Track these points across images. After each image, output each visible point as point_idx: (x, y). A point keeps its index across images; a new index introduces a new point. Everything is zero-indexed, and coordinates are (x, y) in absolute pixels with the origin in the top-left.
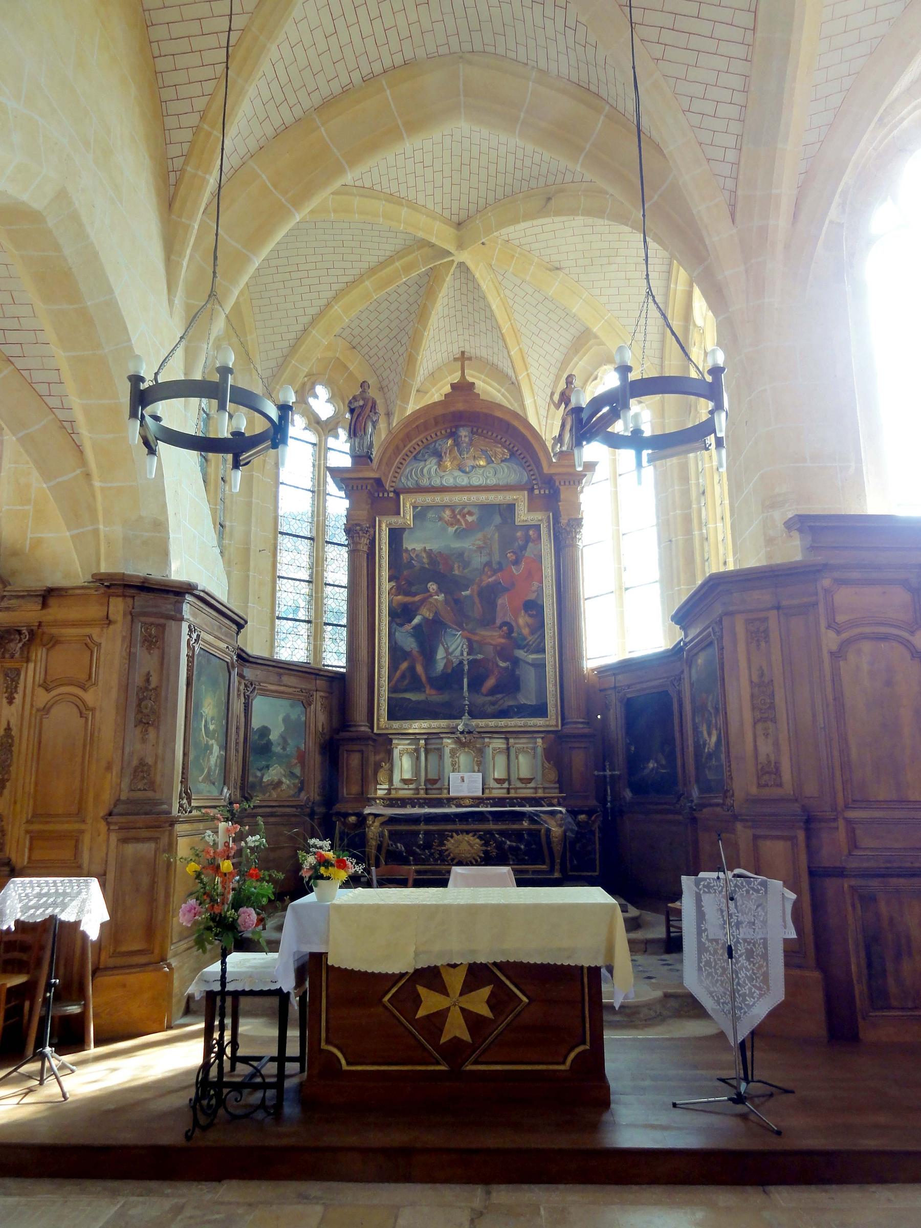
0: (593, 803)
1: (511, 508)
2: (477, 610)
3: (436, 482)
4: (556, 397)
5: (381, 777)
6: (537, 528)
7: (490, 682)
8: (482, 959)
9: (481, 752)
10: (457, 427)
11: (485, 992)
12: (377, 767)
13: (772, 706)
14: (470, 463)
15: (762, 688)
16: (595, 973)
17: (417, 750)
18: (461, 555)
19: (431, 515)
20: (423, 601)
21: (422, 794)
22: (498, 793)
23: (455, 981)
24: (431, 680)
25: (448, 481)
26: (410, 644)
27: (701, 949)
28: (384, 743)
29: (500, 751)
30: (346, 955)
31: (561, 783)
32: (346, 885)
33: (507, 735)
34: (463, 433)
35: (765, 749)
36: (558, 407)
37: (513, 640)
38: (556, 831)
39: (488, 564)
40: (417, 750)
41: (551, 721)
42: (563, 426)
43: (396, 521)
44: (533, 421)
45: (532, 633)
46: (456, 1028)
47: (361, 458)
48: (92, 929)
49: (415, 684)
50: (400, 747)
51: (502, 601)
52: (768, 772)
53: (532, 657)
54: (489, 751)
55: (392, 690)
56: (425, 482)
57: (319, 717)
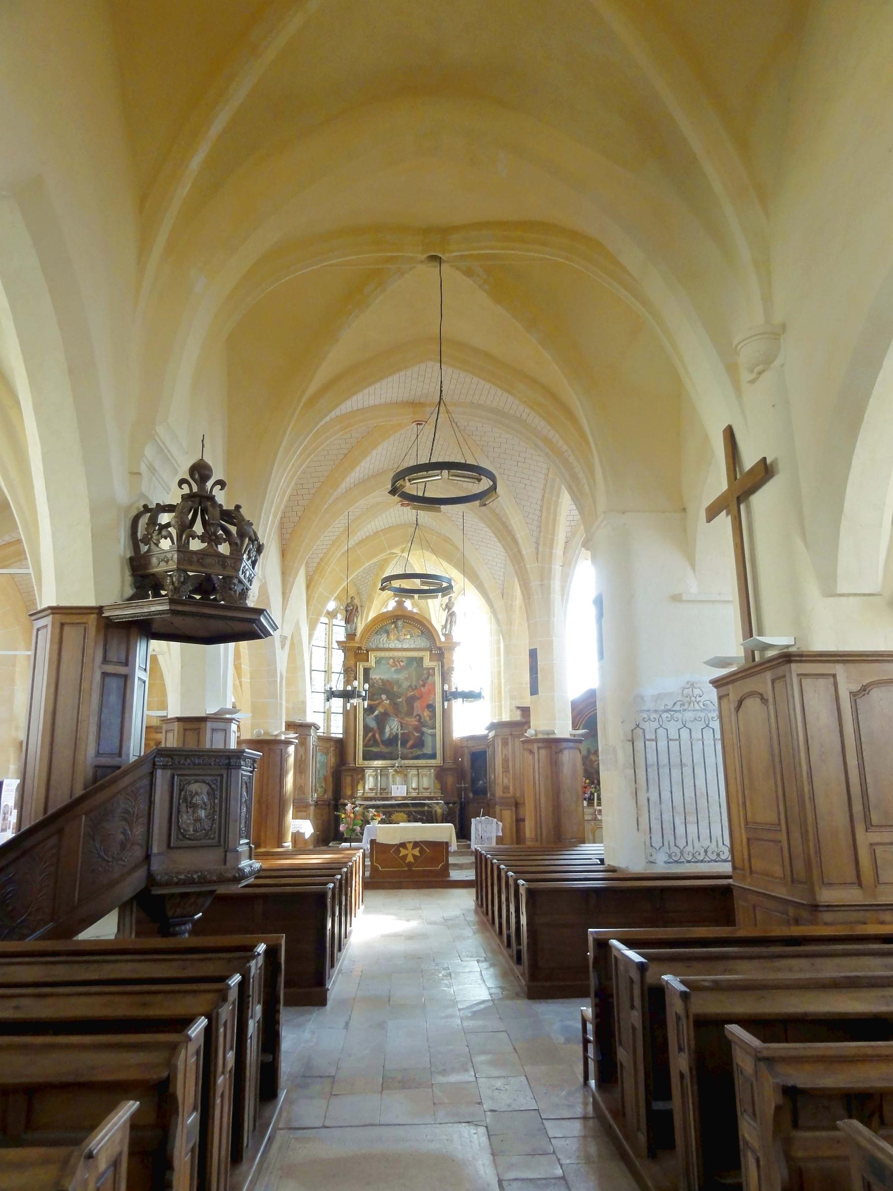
0: (456, 799)
1: (421, 659)
2: (404, 708)
3: (386, 646)
4: (444, 606)
5: (360, 787)
6: (434, 669)
7: (411, 743)
8: (417, 840)
9: (406, 776)
10: (398, 619)
11: (418, 849)
12: (358, 783)
13: (508, 767)
14: (402, 637)
15: (505, 761)
16: (447, 843)
17: (376, 775)
18: (397, 682)
19: (383, 661)
20: (379, 704)
21: (379, 795)
22: (414, 794)
23: (410, 846)
24: (383, 742)
25: (392, 645)
26: (373, 724)
27: (476, 838)
28: (362, 770)
29: (413, 775)
30: (380, 840)
31: (443, 789)
32: (380, 822)
33: (418, 768)
34: (400, 623)
35: (506, 781)
36: (444, 610)
37: (421, 723)
38: (439, 811)
39: (410, 686)
40: (376, 775)
41: (438, 762)
42: (447, 621)
43: (366, 664)
44: (434, 622)
45: (430, 719)
46: (410, 859)
47: (351, 636)
48: (307, 836)
49: (376, 743)
50: (368, 772)
51: (417, 704)
52: (506, 789)
53: (430, 731)
54: (410, 775)
55: (365, 746)
56: (381, 646)
57: (332, 760)
